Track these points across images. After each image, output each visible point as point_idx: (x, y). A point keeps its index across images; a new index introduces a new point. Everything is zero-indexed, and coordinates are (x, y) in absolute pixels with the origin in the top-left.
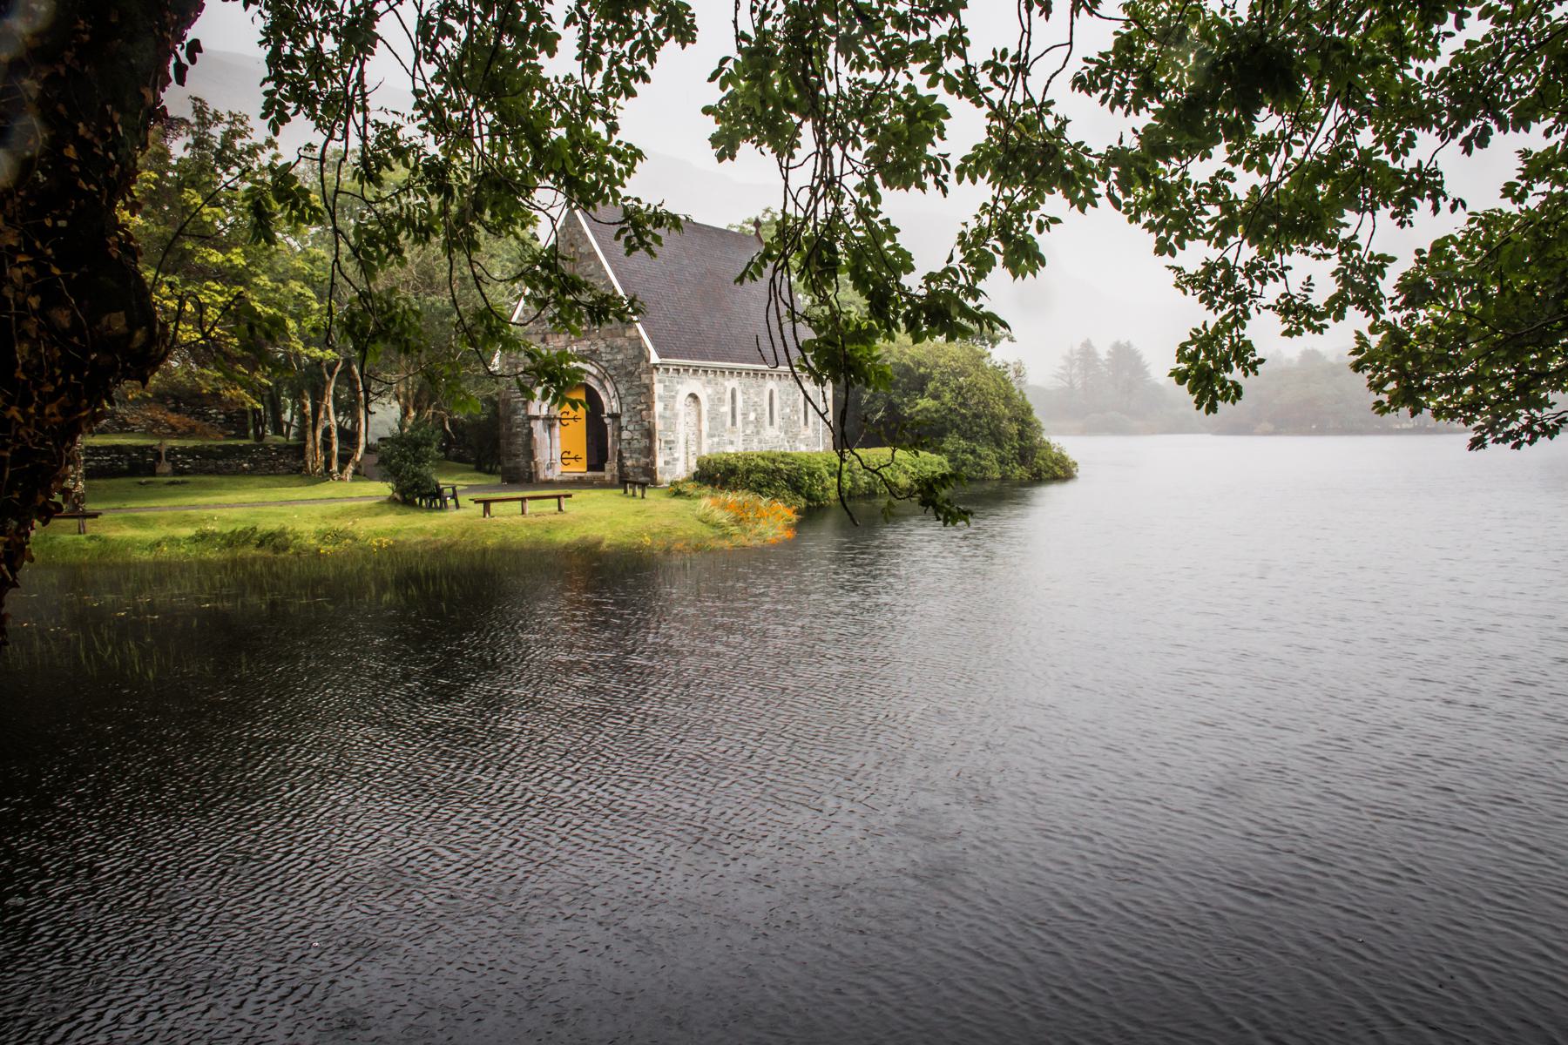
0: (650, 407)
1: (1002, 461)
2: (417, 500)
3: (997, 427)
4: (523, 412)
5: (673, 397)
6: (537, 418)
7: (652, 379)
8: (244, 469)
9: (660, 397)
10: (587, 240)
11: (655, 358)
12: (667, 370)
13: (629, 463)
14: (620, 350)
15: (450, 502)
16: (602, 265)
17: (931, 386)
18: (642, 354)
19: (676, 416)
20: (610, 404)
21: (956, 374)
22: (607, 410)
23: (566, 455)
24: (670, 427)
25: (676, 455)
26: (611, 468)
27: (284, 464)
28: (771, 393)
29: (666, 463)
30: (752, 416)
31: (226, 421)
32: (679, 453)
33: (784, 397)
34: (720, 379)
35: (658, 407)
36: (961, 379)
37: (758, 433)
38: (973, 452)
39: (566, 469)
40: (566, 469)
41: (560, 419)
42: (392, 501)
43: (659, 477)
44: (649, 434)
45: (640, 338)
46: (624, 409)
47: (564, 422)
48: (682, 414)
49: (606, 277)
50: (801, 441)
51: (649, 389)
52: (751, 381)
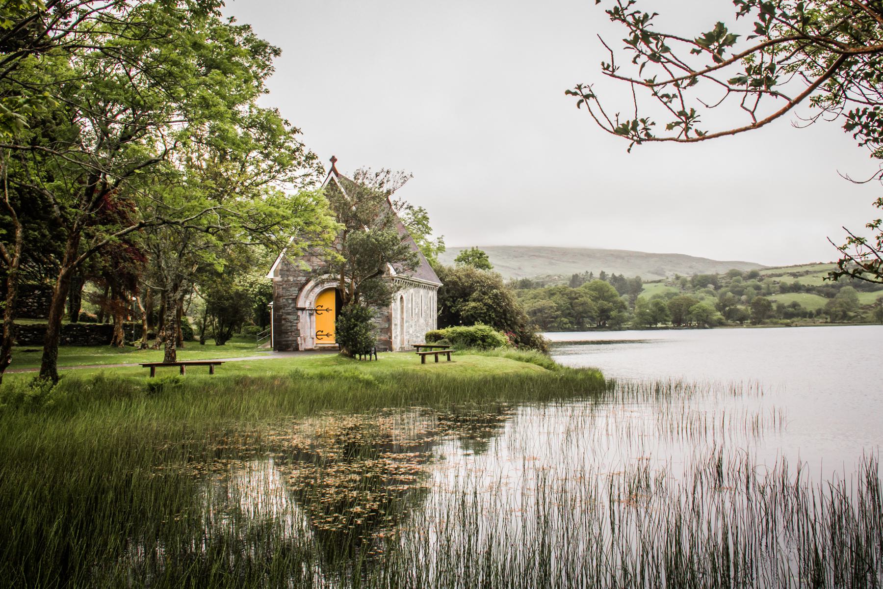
3: (515, 319)
4: (292, 305)
6: (303, 309)
8: (67, 342)
17: (475, 295)
23: (320, 333)
27: (94, 338)
31: (38, 308)
39: (319, 342)
40: (319, 342)
41: (316, 310)
47: (319, 312)
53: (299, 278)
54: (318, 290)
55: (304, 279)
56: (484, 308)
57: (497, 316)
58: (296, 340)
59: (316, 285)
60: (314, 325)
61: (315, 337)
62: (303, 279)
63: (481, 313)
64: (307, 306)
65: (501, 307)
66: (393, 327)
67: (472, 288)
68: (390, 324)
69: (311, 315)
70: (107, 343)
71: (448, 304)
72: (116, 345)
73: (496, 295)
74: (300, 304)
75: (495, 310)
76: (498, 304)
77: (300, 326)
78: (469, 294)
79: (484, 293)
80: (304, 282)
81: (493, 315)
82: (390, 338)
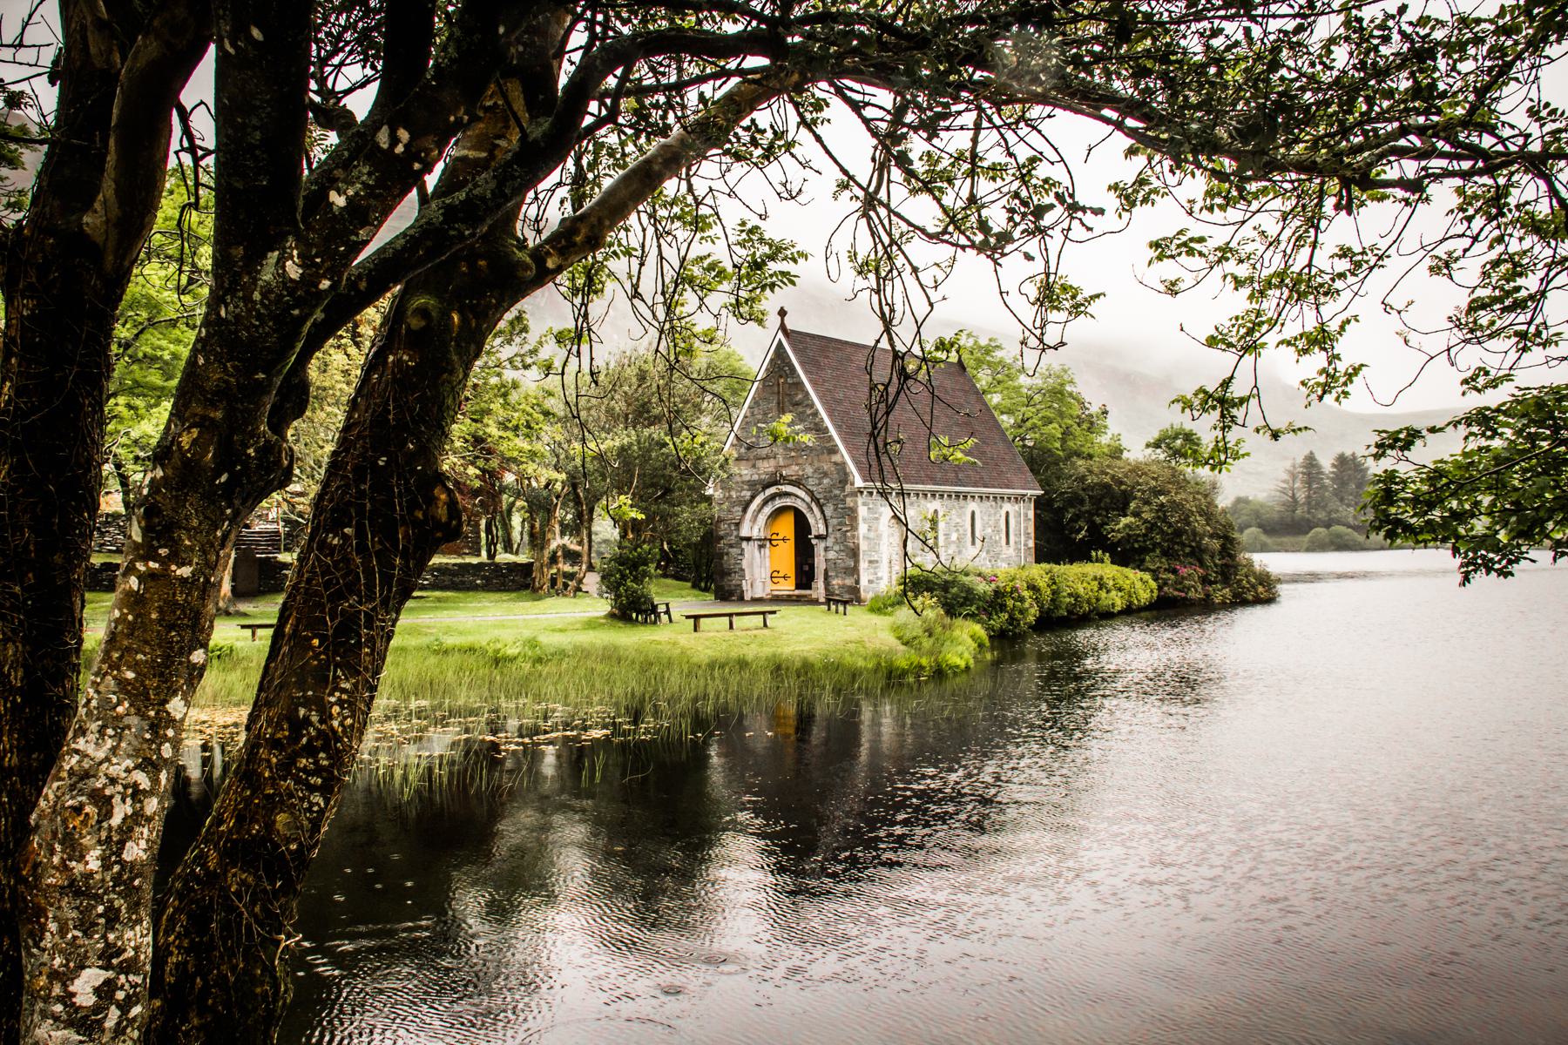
0: (854, 528)
1: (1205, 580)
2: (634, 615)
3: (1199, 543)
4: (735, 533)
5: (877, 519)
6: (748, 539)
7: (856, 502)
9: (864, 520)
10: (793, 369)
11: (859, 482)
12: (871, 494)
13: (834, 582)
14: (825, 475)
15: (664, 617)
16: (807, 394)
17: (1133, 505)
18: (844, 478)
19: (879, 537)
20: (817, 526)
21: (1157, 492)
22: (814, 532)
23: (775, 574)
24: (874, 547)
25: (879, 575)
26: (819, 589)
27: (513, 581)
28: (973, 514)
29: (870, 582)
30: (954, 537)
32: (883, 571)
33: (986, 518)
34: (922, 500)
35: (862, 528)
36: (1161, 498)
37: (960, 552)
38: (1174, 571)
39: (775, 587)
40: (775, 587)
41: (770, 540)
42: (611, 616)
43: (863, 594)
44: (854, 553)
45: (844, 463)
46: (830, 530)
48: (885, 535)
49: (812, 405)
50: (1003, 560)
51: (852, 513)
52: (953, 502)
53: (744, 493)
54: (768, 510)
55: (749, 494)
56: (1143, 527)
57: (1163, 540)
58: (740, 586)
59: (765, 502)
60: (768, 564)
61: (768, 579)
62: (747, 494)
63: (1139, 535)
64: (755, 534)
65: (1170, 525)
66: (863, 565)
67: (1126, 498)
68: (857, 562)
69: (761, 547)
70: (526, 587)
71: (1098, 520)
72: (535, 590)
73: (1162, 505)
74: (744, 532)
75: (1162, 532)
76: (1164, 520)
77: (745, 564)
78: (1126, 505)
79: (1147, 502)
80: (748, 498)
81: (1158, 538)
82: (857, 582)
